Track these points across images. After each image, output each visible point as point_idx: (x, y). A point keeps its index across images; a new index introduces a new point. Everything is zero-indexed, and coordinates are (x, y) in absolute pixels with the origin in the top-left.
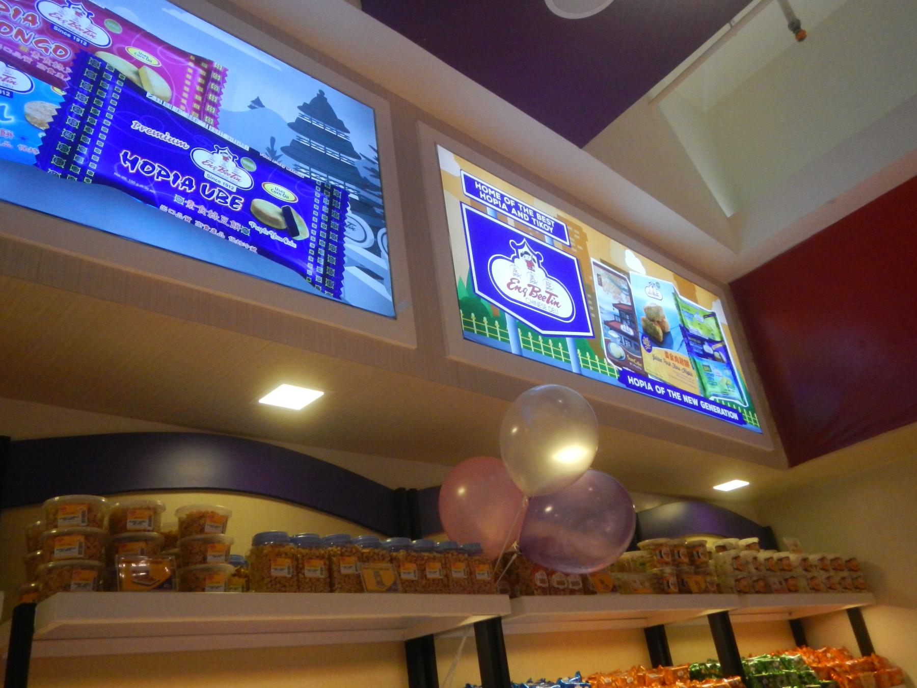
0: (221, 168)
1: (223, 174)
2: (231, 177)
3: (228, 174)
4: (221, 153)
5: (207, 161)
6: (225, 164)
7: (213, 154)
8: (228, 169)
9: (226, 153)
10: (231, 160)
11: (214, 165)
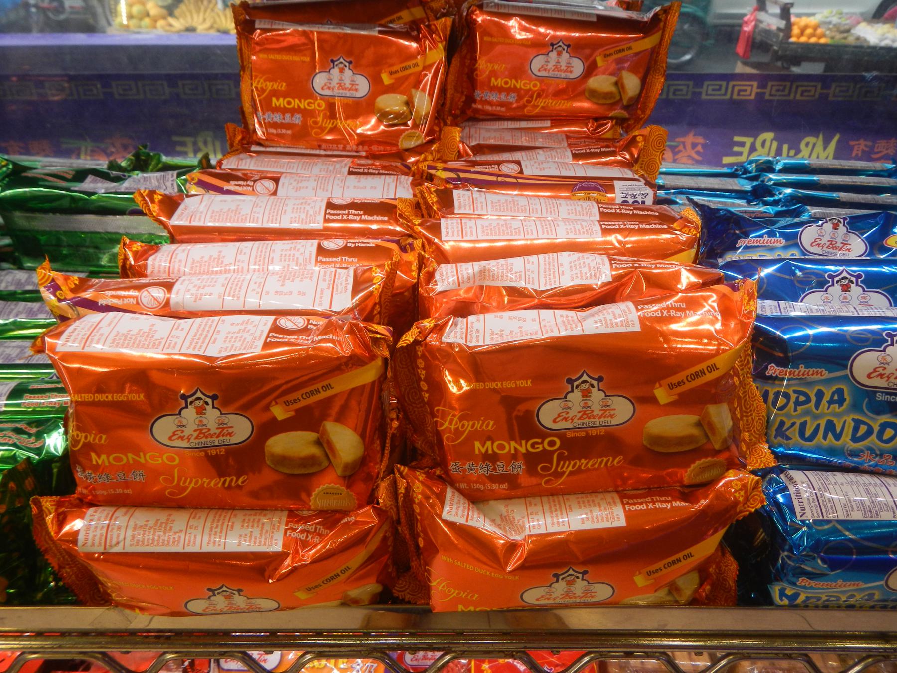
2: (218, 437)
5: (174, 434)
8: (209, 426)
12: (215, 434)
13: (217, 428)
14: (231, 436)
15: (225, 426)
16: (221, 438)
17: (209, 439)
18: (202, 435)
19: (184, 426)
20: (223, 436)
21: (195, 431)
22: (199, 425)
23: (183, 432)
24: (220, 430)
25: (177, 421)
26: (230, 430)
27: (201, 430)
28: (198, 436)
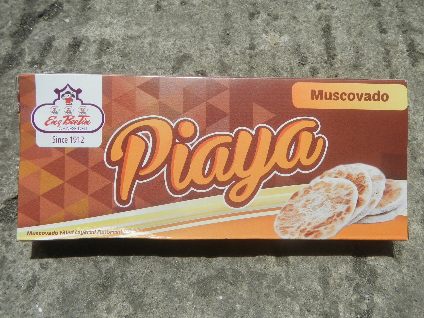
0: (66, 118)
1: (69, 125)
2: (79, 124)
3: (74, 122)
4: (63, 96)
6: (69, 109)
7: (54, 104)
9: (68, 92)
10: (74, 99)
11: (58, 119)
12: (77, 121)
13: (79, 116)
14: (87, 124)
15: (84, 115)
16: (81, 125)
17: (73, 125)
18: (68, 121)
19: (57, 113)
20: (82, 123)
21: (64, 117)
22: (67, 113)
23: (56, 117)
24: (81, 118)
25: (52, 110)
26: (88, 119)
27: (68, 116)
28: (65, 122)
